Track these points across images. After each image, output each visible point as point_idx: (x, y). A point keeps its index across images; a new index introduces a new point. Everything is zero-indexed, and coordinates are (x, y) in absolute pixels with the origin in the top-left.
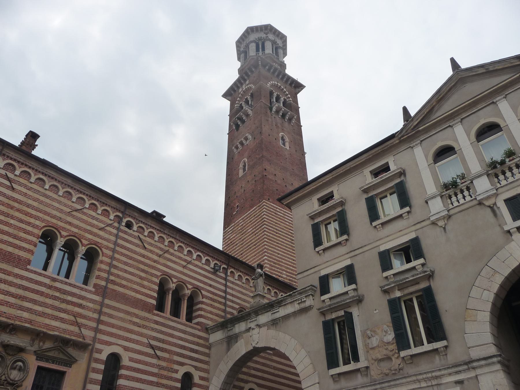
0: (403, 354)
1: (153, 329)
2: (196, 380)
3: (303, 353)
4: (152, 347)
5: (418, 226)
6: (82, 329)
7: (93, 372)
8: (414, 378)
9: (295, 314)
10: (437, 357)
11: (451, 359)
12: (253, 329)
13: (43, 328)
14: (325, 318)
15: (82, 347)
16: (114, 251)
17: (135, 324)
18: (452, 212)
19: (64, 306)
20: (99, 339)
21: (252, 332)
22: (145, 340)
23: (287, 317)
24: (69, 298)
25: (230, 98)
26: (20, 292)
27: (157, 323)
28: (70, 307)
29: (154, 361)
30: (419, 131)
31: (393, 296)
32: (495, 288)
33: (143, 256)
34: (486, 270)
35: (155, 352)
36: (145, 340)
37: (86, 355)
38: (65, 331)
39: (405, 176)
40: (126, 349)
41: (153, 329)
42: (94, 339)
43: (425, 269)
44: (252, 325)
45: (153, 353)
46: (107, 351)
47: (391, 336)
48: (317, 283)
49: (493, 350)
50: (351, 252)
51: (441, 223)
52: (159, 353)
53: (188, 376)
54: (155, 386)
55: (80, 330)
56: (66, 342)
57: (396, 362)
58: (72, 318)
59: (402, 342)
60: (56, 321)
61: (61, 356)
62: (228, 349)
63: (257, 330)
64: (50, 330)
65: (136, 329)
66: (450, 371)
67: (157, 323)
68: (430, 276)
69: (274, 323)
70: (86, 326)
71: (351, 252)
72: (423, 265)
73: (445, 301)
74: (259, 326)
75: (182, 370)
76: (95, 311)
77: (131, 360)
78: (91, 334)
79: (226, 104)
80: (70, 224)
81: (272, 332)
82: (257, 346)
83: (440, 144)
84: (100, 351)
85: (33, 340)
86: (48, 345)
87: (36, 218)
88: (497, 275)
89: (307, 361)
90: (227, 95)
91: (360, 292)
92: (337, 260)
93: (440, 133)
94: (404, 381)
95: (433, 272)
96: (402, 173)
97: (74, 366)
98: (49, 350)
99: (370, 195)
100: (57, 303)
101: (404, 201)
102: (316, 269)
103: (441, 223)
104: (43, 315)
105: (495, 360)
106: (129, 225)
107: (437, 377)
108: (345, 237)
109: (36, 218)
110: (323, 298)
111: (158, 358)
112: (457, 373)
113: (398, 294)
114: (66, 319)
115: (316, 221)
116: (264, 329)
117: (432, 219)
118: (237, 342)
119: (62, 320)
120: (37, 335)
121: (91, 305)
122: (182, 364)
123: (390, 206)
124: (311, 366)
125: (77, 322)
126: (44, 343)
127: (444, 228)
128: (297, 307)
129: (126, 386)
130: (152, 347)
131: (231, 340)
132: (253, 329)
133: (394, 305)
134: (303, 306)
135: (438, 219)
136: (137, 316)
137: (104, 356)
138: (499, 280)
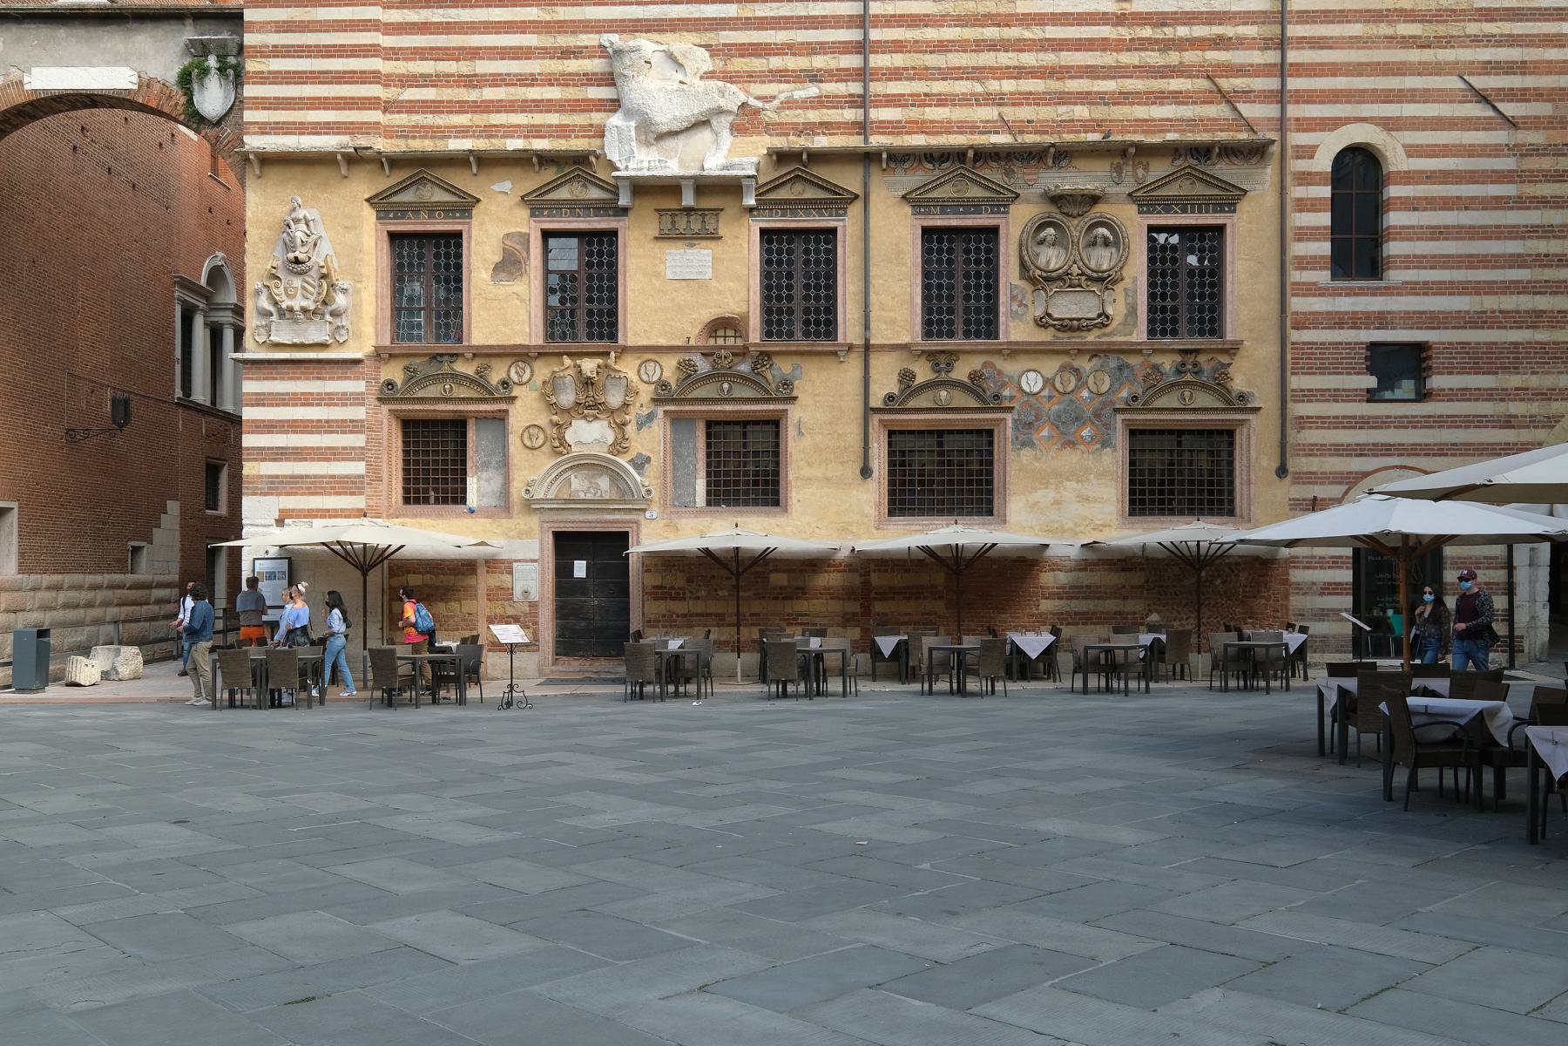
1: (1476, 41)
4: (1483, 98)
6: (1240, 106)
7: (1301, 211)
13: (1135, 132)
15: (1255, 152)
17: (1407, 42)
19: (1173, 58)
20: (1297, 119)
22: (1454, 83)
24: (1182, 31)
26: (1049, 58)
28: (1191, 57)
29: (1500, 137)
35: (1495, 108)
36: (1454, 83)
37: (1270, 172)
38: (1192, 123)
40: (1390, 124)
41: (1476, 41)
42: (1282, 124)
45: (1490, 113)
46: (1328, 147)
52: (1509, 109)
54: (1512, 208)
55: (1236, 109)
56: (1202, 152)
58: (1203, 84)
60: (1162, 104)
61: (1200, 189)
64: (1153, 132)
65: (1414, 55)
70: (1247, 95)
76: (1265, 44)
77: (1413, 151)
78: (1272, 111)
84: (1308, 152)
85: (1118, 169)
97: (1244, 206)
98: (1165, 181)
100: (1153, 58)
104: (1124, 98)
111: (1512, 123)
114: (1188, 91)
119: (1178, 98)
121: (1250, 31)
125: (1220, 91)
126: (1146, 168)
129: (1412, 227)
130: (1483, 98)
137: (1323, 163)
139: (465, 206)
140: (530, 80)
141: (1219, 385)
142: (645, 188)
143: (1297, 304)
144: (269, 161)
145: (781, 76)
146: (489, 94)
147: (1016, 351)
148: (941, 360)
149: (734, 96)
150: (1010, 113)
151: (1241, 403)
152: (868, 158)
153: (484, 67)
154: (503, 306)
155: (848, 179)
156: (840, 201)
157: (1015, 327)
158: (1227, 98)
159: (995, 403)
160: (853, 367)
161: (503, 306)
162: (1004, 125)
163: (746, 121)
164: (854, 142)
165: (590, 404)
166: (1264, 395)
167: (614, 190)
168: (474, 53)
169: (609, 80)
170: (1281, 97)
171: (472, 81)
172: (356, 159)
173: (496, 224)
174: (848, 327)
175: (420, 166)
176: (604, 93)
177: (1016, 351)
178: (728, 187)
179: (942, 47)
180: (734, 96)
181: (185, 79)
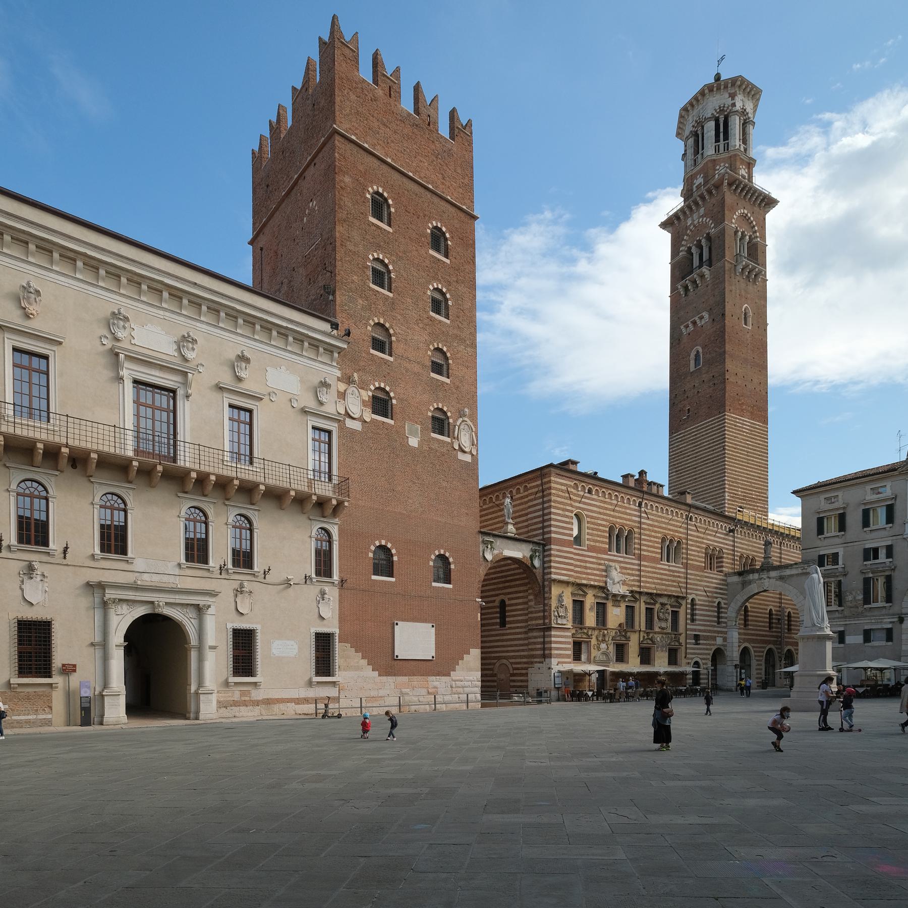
2: (723, 605)
15: (683, 598)
16: (687, 539)
25: (670, 229)
27: (706, 577)
33: (698, 537)
53: (719, 603)
56: (678, 597)
62: (743, 588)
67: (706, 577)
75: (717, 601)
79: (666, 237)
80: (670, 530)
86: (673, 600)
87: (659, 532)
90: (665, 225)
104: (668, 586)
106: (691, 519)
109: (659, 532)
120: (669, 596)
122: (717, 598)
131: (744, 584)
136: (698, 575)
139: (585, 594)
140: (594, 569)
141: (678, 641)
142: (615, 595)
143: (688, 627)
144: (554, 580)
145: (629, 574)
146: (589, 571)
147: (655, 633)
148: (648, 634)
149: (624, 577)
150: (658, 587)
151: (680, 644)
152: (640, 593)
153: (588, 565)
154: (590, 619)
155: (637, 596)
156: (636, 600)
157: (657, 629)
158: (680, 587)
159: (654, 643)
160: (637, 634)
161: (590, 619)
162: (656, 589)
163: (624, 583)
164: (638, 589)
165: (603, 641)
166: (684, 644)
167: (607, 595)
168: (586, 562)
169: (606, 571)
170: (686, 588)
171: (586, 568)
172: (567, 583)
173: (590, 601)
174: (637, 628)
175: (580, 586)
176: (604, 573)
177: (655, 633)
178: (623, 597)
179: (648, 572)
180: (624, 577)
181: (531, 558)
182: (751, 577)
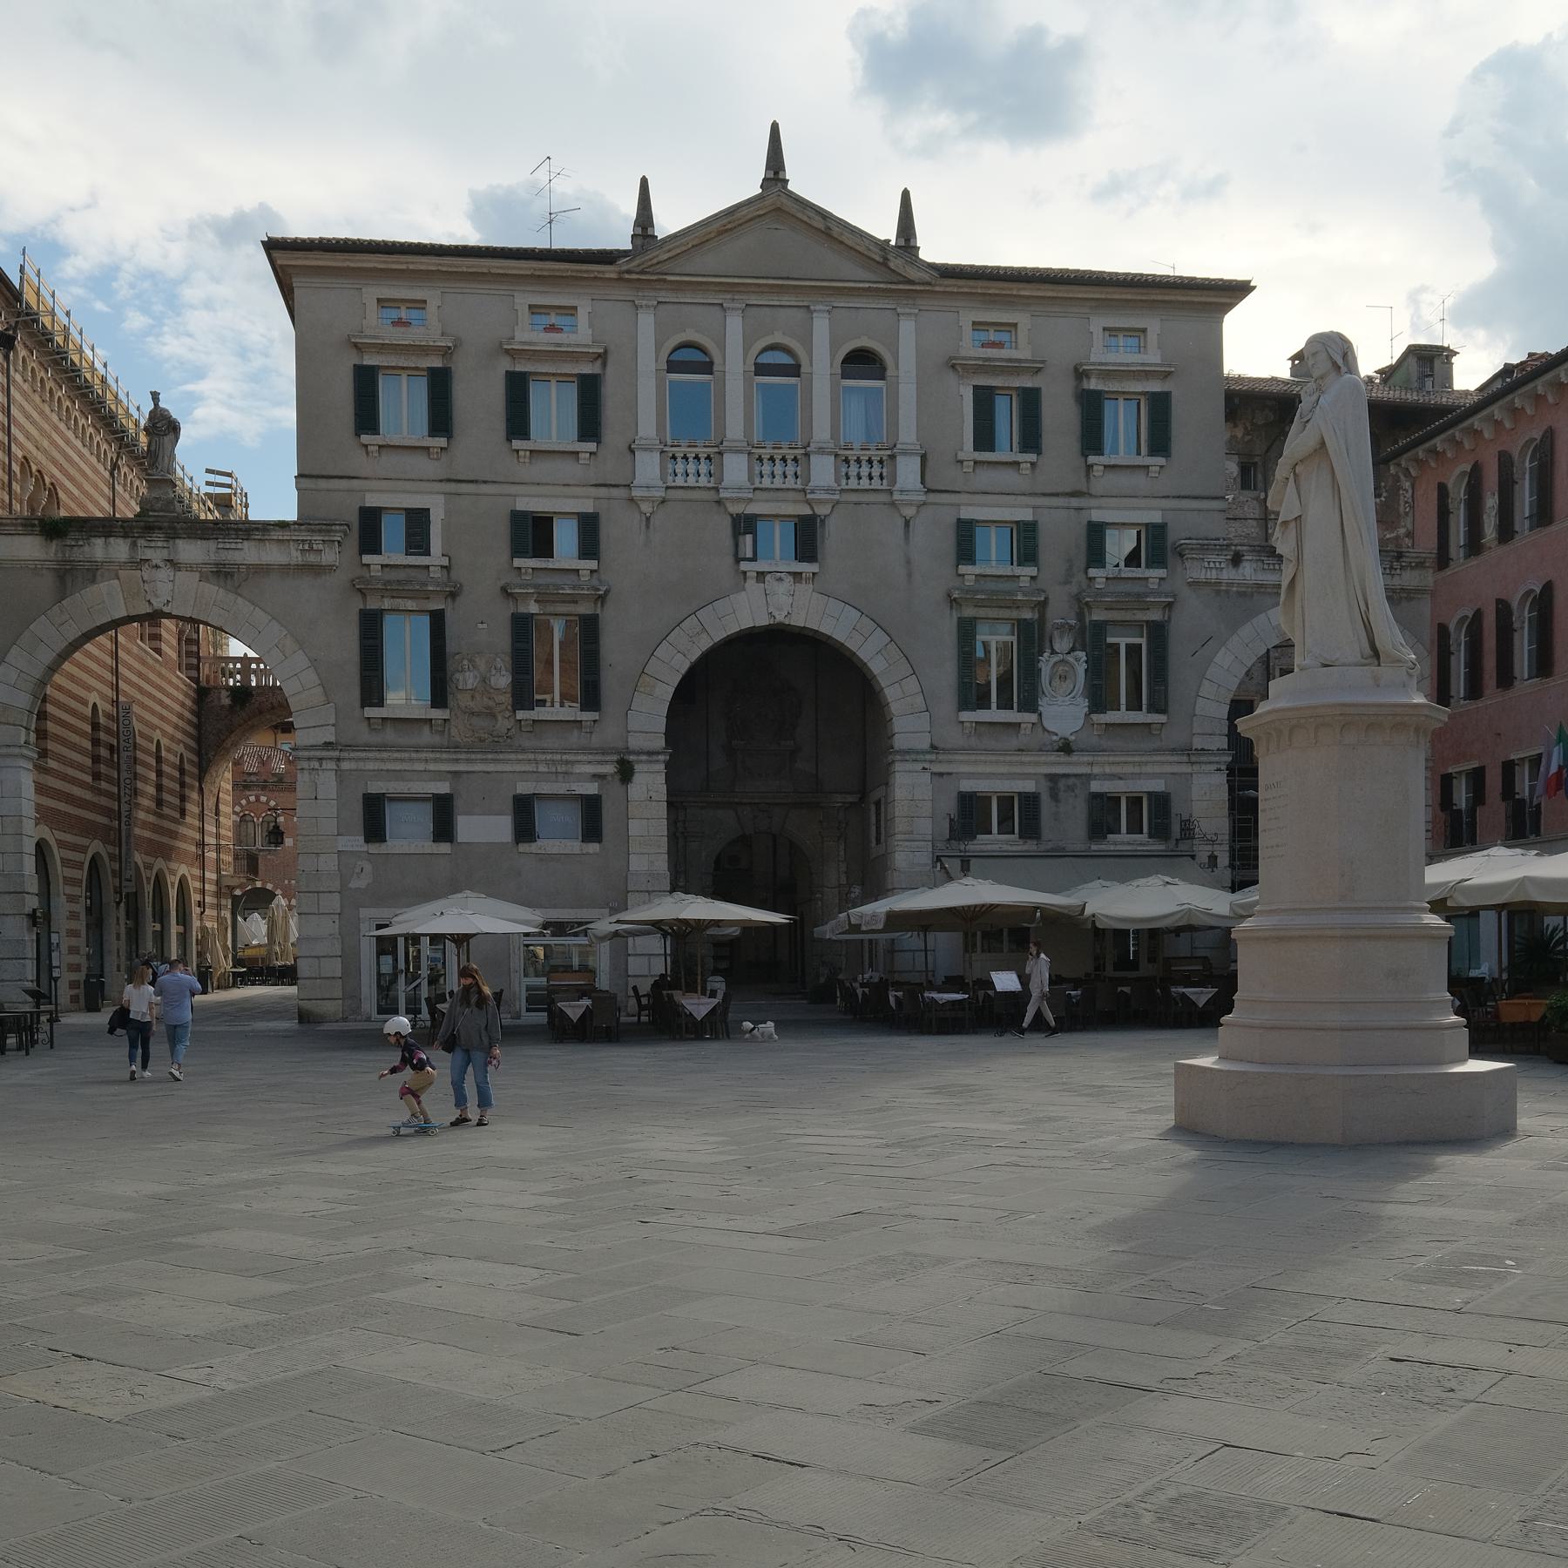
0: (520, 715)
3: (300, 660)
5: (603, 492)
8: (531, 756)
9: (285, 570)
10: (576, 732)
11: (595, 740)
12: (157, 567)
14: (365, 602)
18: (672, 494)
21: (146, 573)
23: (262, 570)
30: (665, 281)
31: (522, 610)
32: (695, 655)
34: (692, 621)
39: (604, 365)
43: (595, 582)
44: (156, 556)
47: (503, 680)
48: (354, 519)
49: (660, 743)
50: (449, 480)
51: (646, 508)
57: (503, 724)
59: (523, 695)
62: (62, 593)
63: (165, 573)
66: (591, 757)
68: (602, 599)
69: (222, 573)
71: (449, 480)
72: (592, 571)
73: (614, 650)
74: (173, 564)
81: (211, 590)
82: (166, 610)
83: (690, 335)
88: (704, 635)
89: (311, 677)
91: (454, 575)
92: (408, 485)
93: (700, 308)
94: (512, 756)
95: (607, 592)
96: (603, 357)
99: (519, 368)
101: (590, 427)
102: (355, 483)
103: (646, 508)
105: (661, 757)
107: (567, 762)
108: (442, 442)
110: (367, 559)
112: (600, 763)
113: (533, 608)
115: (369, 361)
116: (188, 580)
117: (636, 493)
118: (93, 581)
123: (554, 413)
124: (320, 689)
127: (648, 519)
128: (295, 556)
132: (157, 567)
133: (522, 628)
134: (312, 558)
135: (644, 499)
138: (705, 644)
182: (98, 549)
